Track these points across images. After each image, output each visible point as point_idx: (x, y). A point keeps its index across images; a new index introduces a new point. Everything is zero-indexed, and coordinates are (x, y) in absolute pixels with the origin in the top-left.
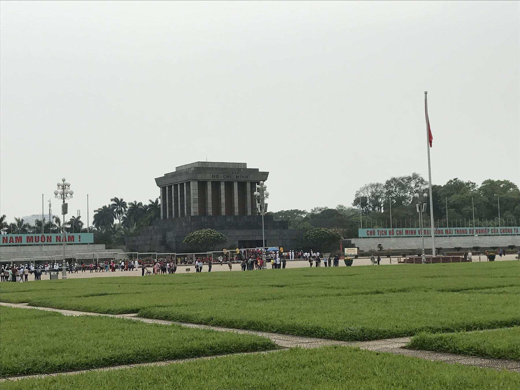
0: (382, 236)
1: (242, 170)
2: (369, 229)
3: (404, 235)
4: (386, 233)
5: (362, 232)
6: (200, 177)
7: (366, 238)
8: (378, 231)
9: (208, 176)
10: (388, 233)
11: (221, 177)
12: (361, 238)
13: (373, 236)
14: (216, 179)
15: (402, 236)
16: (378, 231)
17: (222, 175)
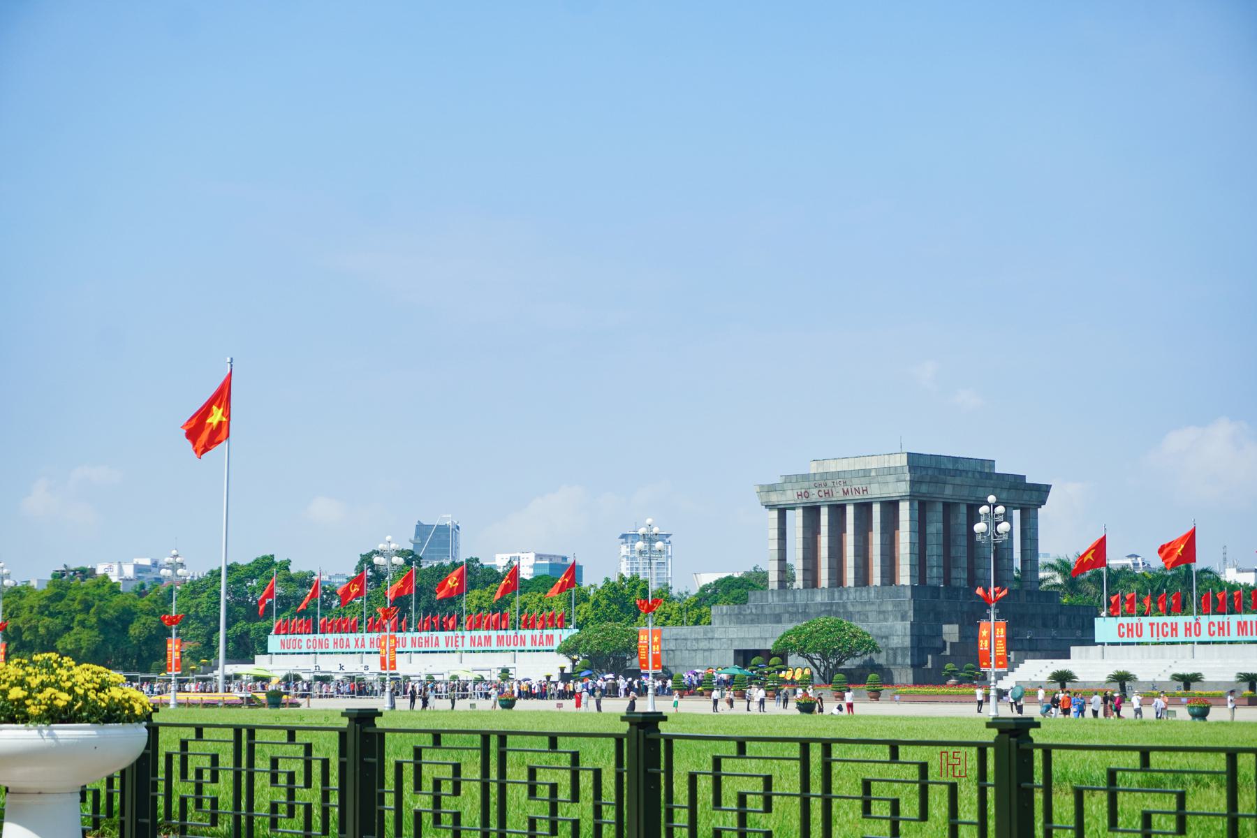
0: (1162, 639)
1: (873, 474)
2: (1126, 620)
3: (1234, 637)
4: (1174, 629)
5: (1105, 627)
6: (775, 498)
7: (1117, 644)
8: (1152, 625)
9: (789, 497)
10: (1181, 630)
11: (814, 497)
12: (1103, 644)
13: (1136, 639)
14: (805, 500)
15: (1226, 638)
16: (1152, 625)
17: (815, 491)
